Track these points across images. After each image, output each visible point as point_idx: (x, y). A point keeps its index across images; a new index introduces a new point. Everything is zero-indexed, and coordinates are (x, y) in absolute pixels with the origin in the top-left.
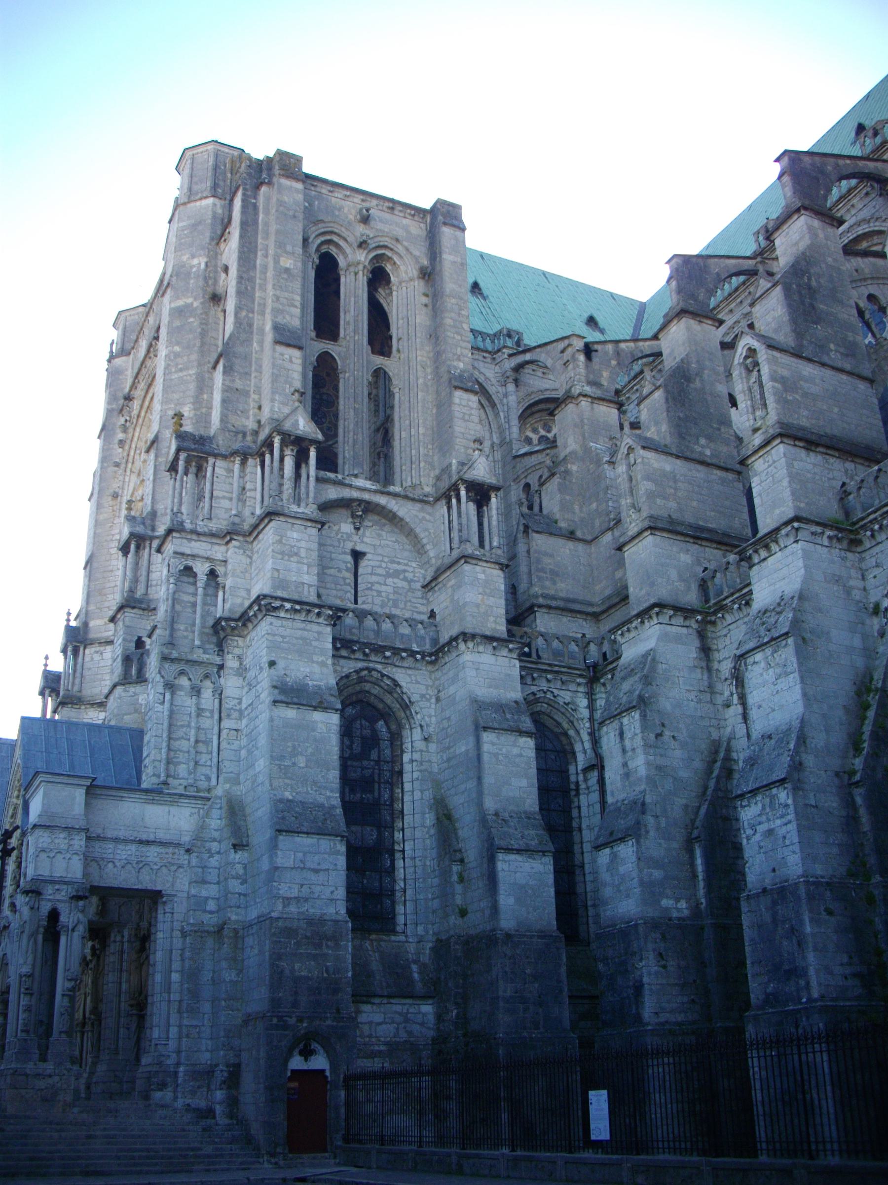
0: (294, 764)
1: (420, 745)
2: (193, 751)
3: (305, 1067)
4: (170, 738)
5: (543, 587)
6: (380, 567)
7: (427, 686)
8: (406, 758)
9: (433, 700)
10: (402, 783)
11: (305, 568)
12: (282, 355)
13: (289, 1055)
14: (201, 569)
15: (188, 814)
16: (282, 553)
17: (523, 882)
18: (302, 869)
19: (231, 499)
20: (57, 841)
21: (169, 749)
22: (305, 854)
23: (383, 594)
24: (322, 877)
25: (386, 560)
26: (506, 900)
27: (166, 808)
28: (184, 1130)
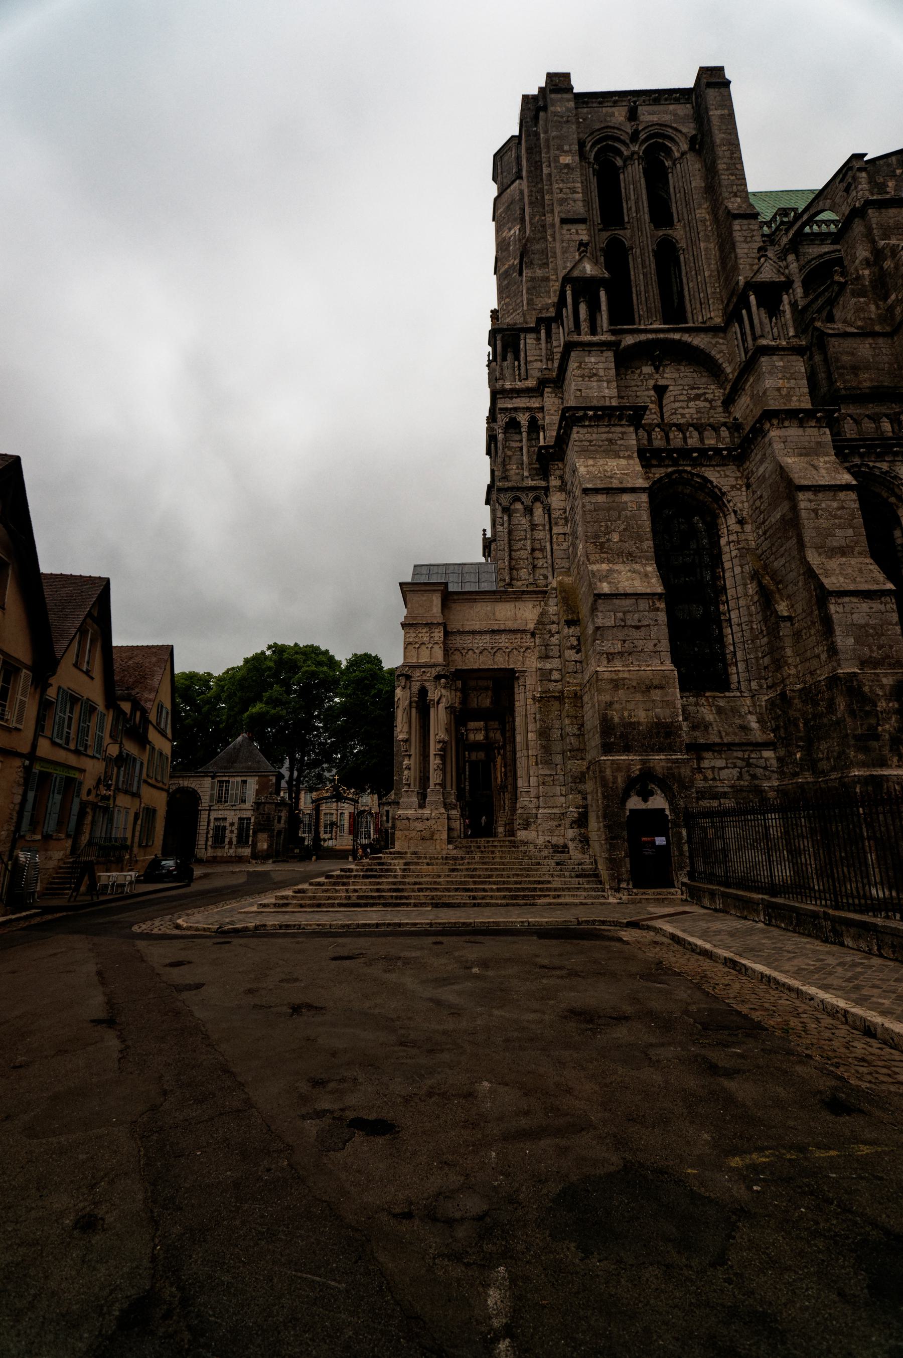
0: (609, 540)
1: (736, 528)
2: (530, 557)
3: (642, 806)
4: (511, 551)
5: (845, 382)
6: (682, 394)
7: (736, 478)
8: (723, 541)
9: (744, 489)
10: (722, 563)
11: (605, 384)
12: (569, 230)
13: (626, 796)
14: (523, 419)
15: (531, 606)
16: (583, 376)
17: (863, 622)
18: (623, 627)
19: (541, 361)
20: (420, 635)
21: (511, 559)
22: (624, 613)
23: (687, 416)
24: (642, 633)
25: (686, 388)
26: (844, 641)
27: (512, 605)
28: (539, 864)
